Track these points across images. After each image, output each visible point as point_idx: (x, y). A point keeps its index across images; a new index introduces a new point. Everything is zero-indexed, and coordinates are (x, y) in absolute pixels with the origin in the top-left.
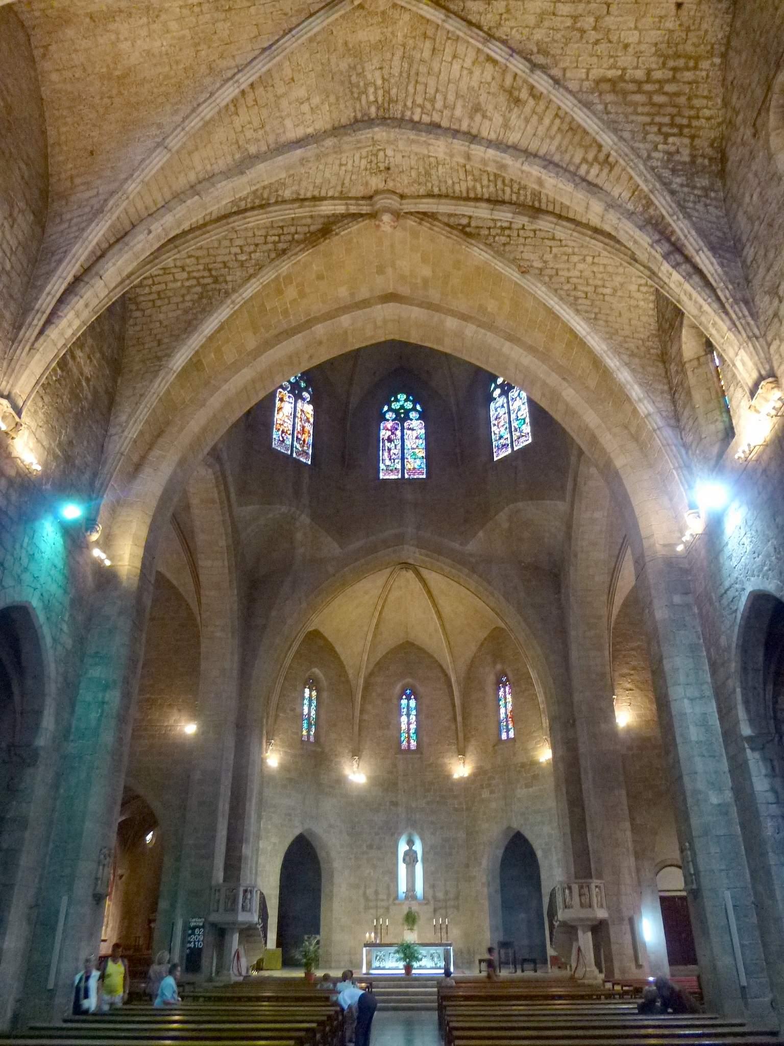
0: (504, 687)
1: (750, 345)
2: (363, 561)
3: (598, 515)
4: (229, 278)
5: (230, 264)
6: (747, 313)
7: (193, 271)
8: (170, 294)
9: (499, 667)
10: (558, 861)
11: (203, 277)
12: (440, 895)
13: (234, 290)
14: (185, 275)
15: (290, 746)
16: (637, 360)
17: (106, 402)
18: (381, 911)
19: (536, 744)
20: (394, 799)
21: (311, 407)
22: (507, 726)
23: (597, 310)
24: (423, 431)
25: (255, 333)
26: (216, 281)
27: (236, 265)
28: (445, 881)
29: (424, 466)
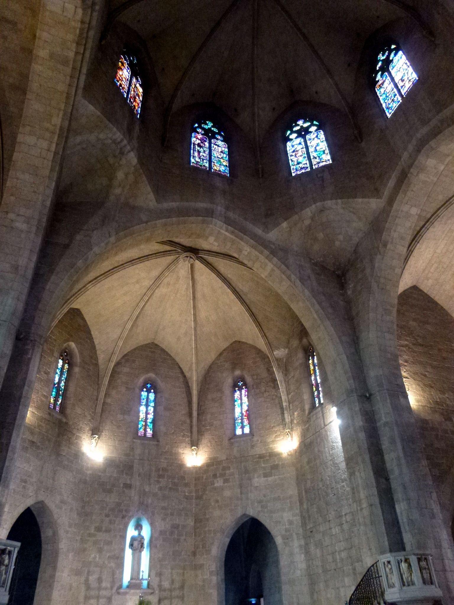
0: (240, 389)
2: (174, 219)
3: (414, 211)
10: (300, 546)
12: (166, 584)
19: (276, 437)
20: (128, 482)
22: (242, 423)
28: (172, 569)
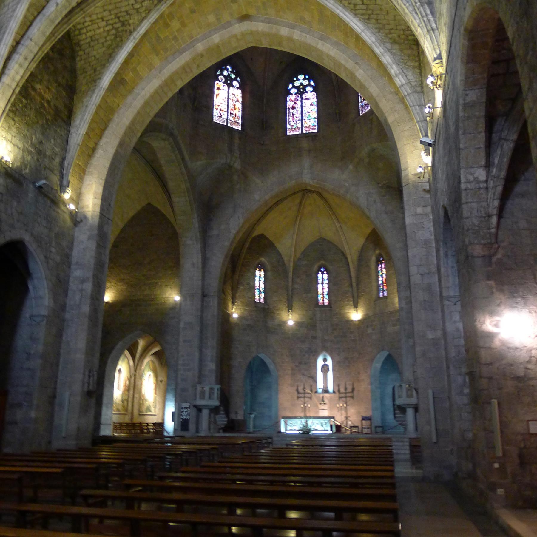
1: (428, 36)
4: (131, 22)
5: (130, 12)
6: (428, 12)
7: (108, 20)
8: (97, 37)
9: (377, 252)
11: (116, 23)
12: (342, 390)
13: (135, 29)
14: (104, 23)
15: (247, 305)
16: (396, 47)
17: (66, 113)
18: (307, 399)
21: (239, 91)
22: (383, 288)
23: (370, 12)
24: (315, 100)
25: (157, 55)
26: (123, 25)
27: (134, 11)
29: (316, 124)
